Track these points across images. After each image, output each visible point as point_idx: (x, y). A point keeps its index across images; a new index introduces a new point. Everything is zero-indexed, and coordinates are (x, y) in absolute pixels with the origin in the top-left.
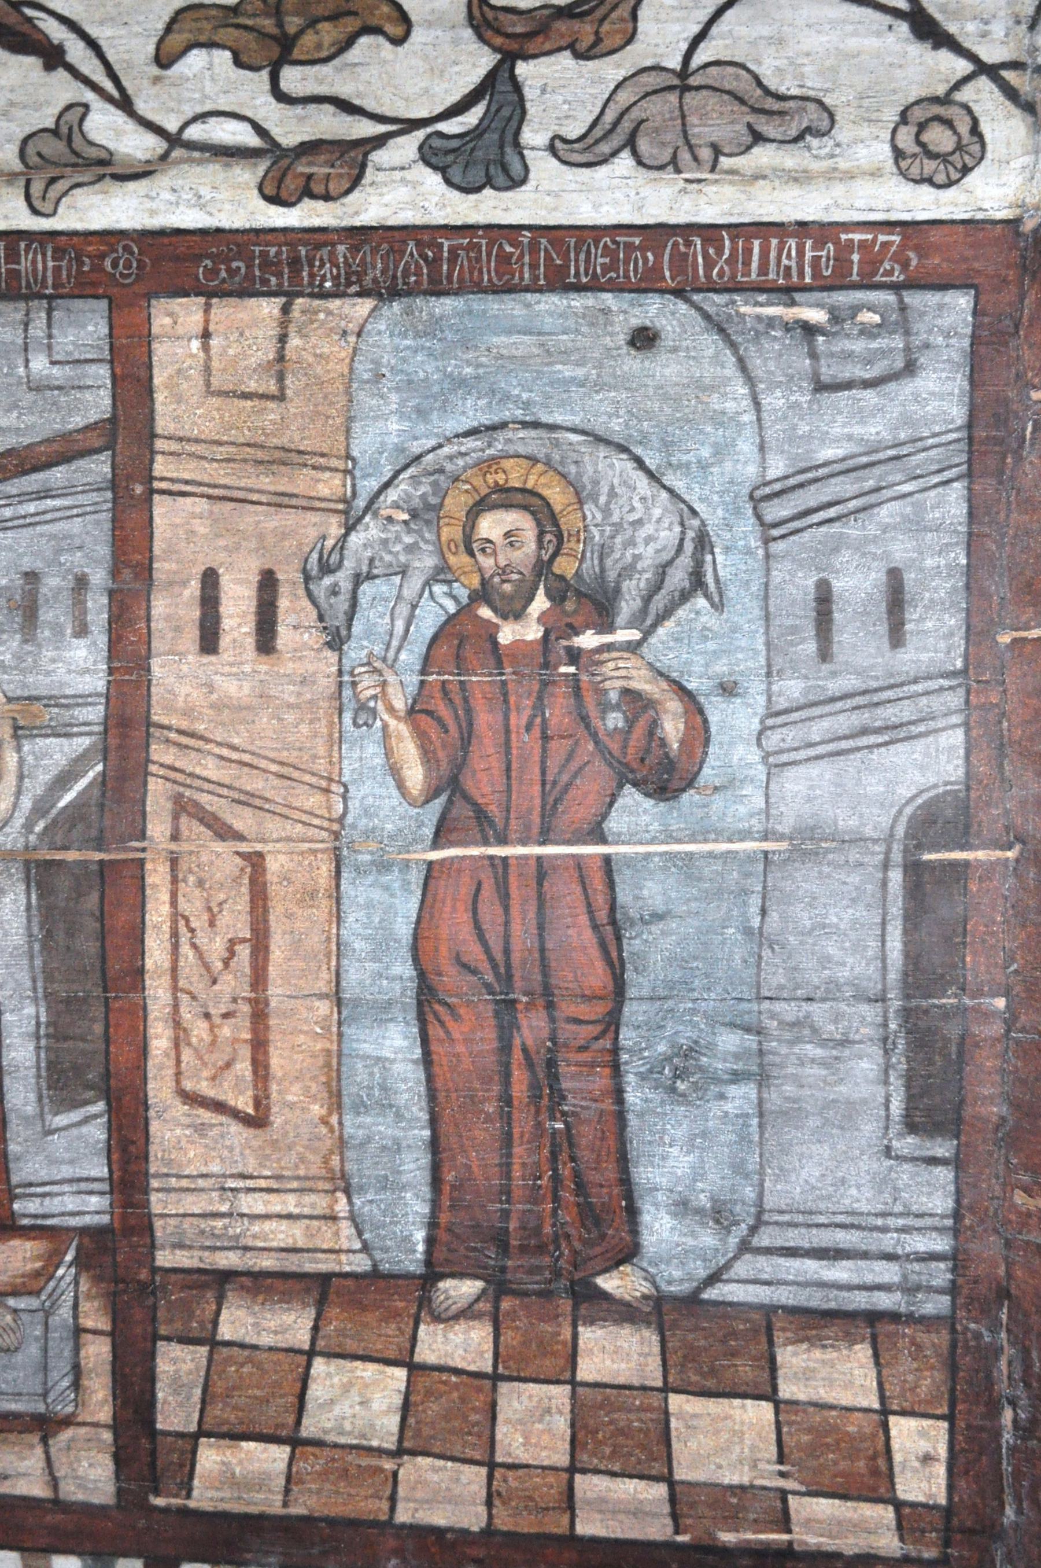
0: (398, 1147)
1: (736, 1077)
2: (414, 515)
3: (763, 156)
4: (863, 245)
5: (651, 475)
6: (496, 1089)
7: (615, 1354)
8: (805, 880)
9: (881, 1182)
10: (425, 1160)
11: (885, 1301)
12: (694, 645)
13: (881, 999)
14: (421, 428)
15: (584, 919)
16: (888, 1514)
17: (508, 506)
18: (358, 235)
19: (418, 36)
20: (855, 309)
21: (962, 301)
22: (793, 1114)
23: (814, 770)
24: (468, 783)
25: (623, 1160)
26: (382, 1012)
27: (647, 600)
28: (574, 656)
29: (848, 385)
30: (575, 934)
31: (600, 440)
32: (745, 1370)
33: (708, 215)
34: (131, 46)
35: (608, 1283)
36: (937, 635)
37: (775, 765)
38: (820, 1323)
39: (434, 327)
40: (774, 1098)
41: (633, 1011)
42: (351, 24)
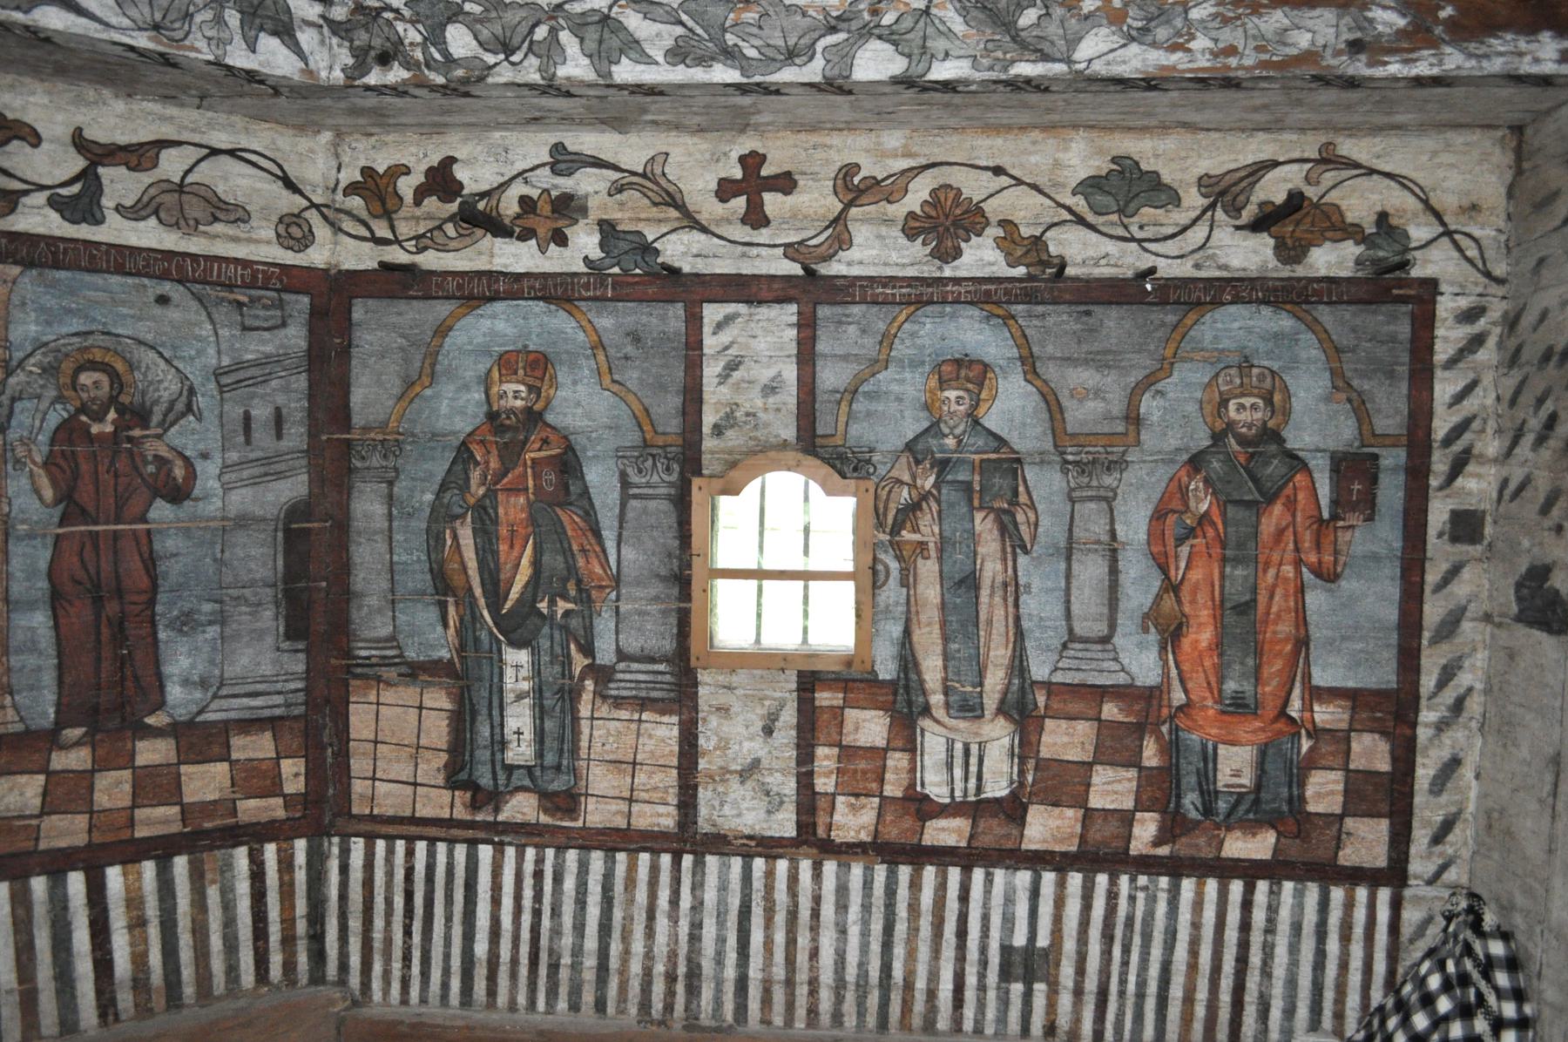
0: (39, 669)
1: (211, 623)
2: (44, 370)
3: (218, 228)
5: (166, 360)
6: (93, 637)
7: (152, 752)
8: (240, 537)
9: (275, 662)
10: (54, 674)
11: (278, 712)
12: (186, 437)
13: (275, 585)
14: (48, 330)
15: (137, 557)
16: (280, 801)
17: (95, 370)
19: (45, 146)
20: (260, 298)
21: (306, 300)
22: (237, 636)
23: (244, 491)
24: (76, 496)
25: (157, 663)
26: (31, 605)
27: (165, 415)
28: (130, 439)
29: (257, 329)
30: (133, 565)
31: (141, 343)
32: (216, 749)
33: (193, 249)
35: (150, 720)
36: (296, 435)
37: (227, 489)
38: (249, 725)
39: (54, 284)
40: (228, 631)
41: (162, 597)
42: (9, 133)
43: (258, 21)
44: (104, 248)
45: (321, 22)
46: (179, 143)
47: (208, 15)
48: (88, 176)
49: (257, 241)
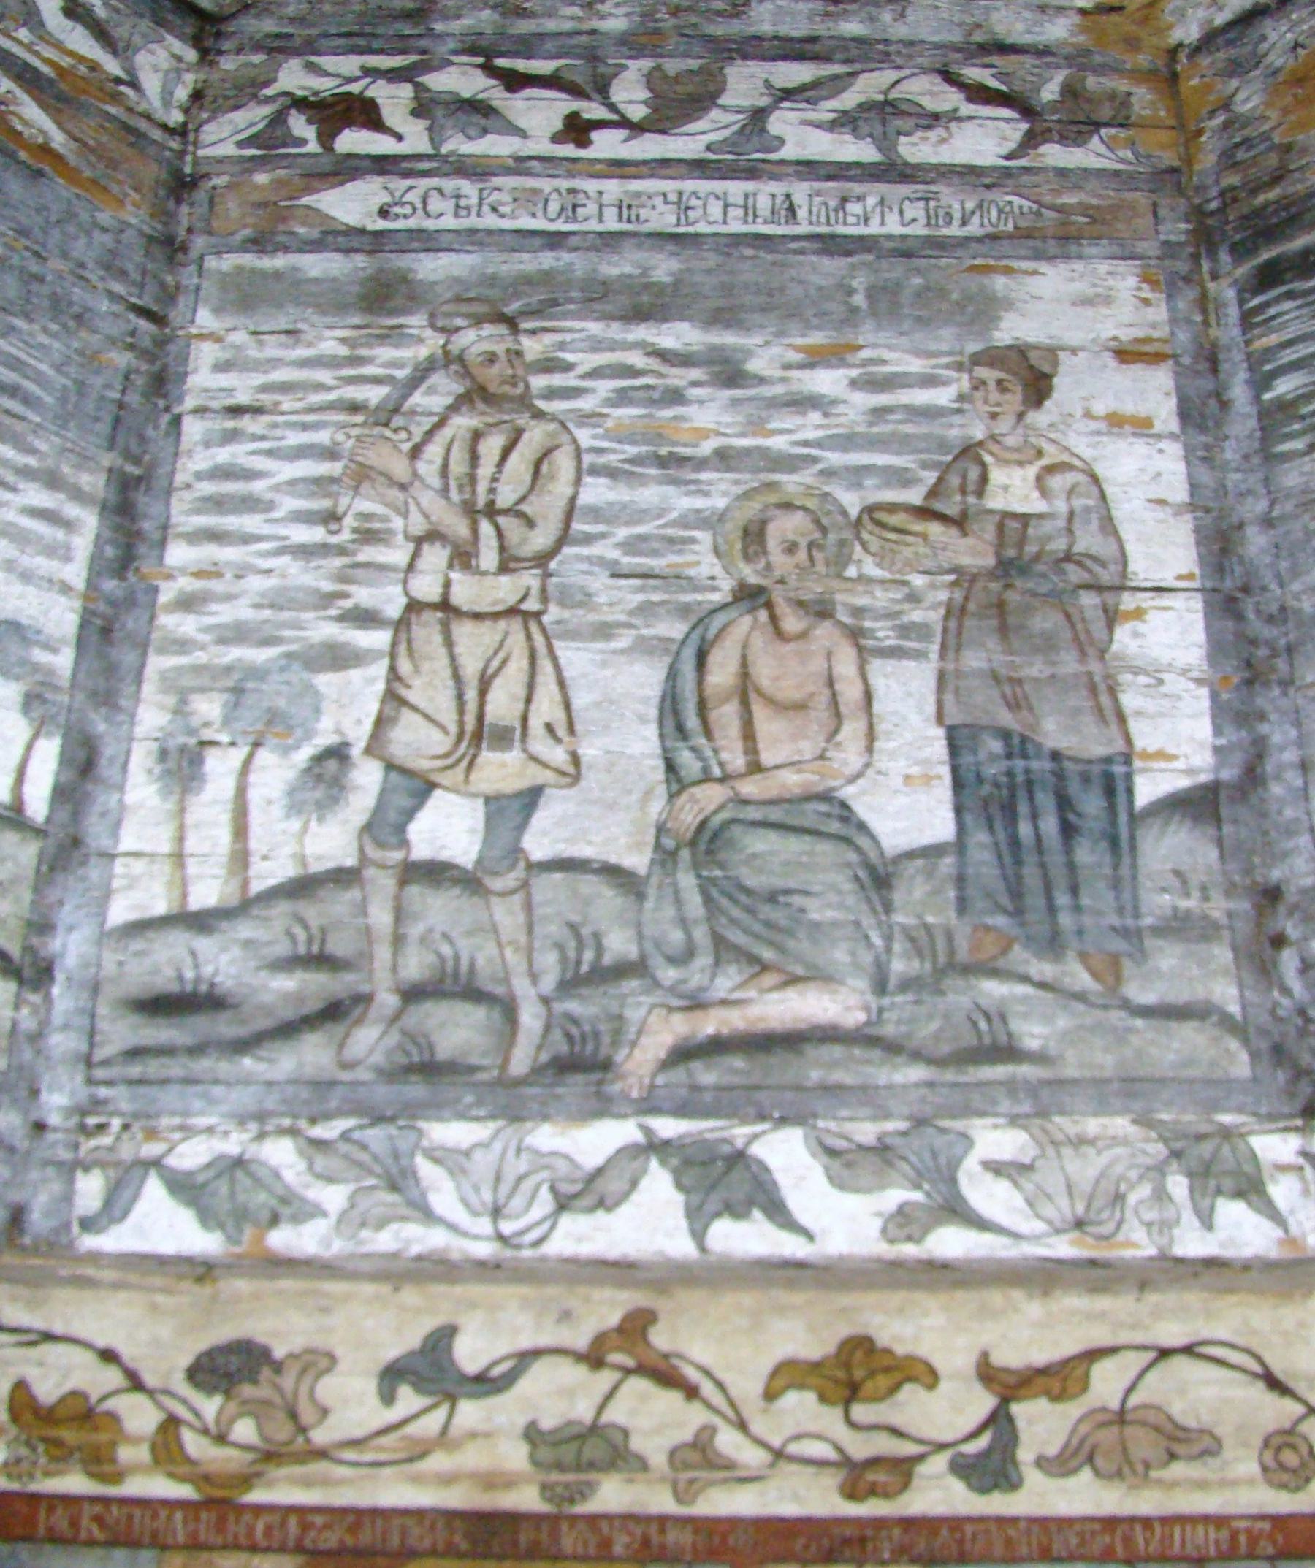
3: (1178, 1470)
4: (1248, 1531)
18: (909, 1523)
19: (944, 1386)
34: (748, 1387)
42: (897, 1376)
43: (1212, 1183)
44: (1022, 1525)
45: (1301, 1161)
46: (1112, 1350)
47: (1145, 1190)
48: (999, 1420)
49: (1234, 1483)
